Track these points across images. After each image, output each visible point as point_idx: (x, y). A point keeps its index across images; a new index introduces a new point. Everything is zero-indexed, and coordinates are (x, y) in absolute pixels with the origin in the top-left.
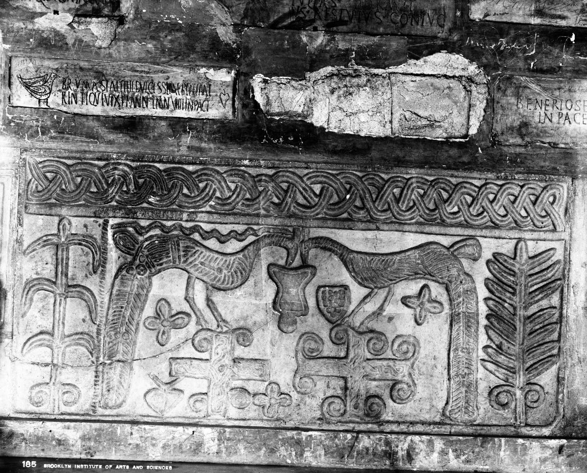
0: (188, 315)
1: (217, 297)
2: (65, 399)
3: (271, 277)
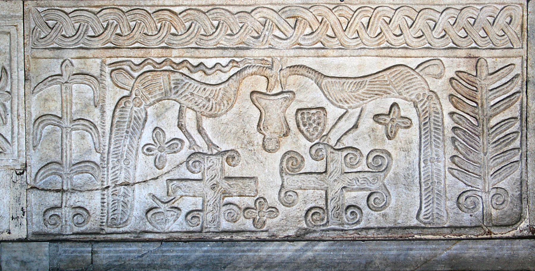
0: (181, 140)
1: (206, 123)
2: (75, 222)
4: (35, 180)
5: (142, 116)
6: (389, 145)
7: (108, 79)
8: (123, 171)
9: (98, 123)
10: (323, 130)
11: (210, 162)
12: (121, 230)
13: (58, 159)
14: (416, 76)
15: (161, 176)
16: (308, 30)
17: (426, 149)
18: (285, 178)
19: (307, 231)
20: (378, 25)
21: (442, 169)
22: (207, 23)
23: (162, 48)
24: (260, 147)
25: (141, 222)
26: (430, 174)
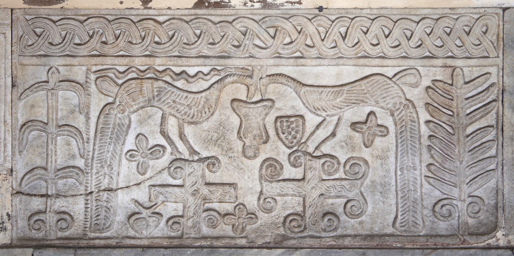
1: (188, 130)
2: (59, 227)
3: (234, 110)
4: (20, 184)
5: (126, 123)
6: (366, 154)
7: (93, 86)
8: (107, 177)
9: (83, 129)
10: (301, 138)
11: (191, 168)
12: (104, 235)
13: (44, 164)
14: (393, 85)
15: (144, 181)
16: (288, 40)
17: (403, 157)
18: (264, 184)
19: (285, 238)
20: (355, 35)
21: (418, 178)
22: (190, 32)
23: (146, 56)
24: (240, 155)
25: (124, 227)
26: (406, 182)
